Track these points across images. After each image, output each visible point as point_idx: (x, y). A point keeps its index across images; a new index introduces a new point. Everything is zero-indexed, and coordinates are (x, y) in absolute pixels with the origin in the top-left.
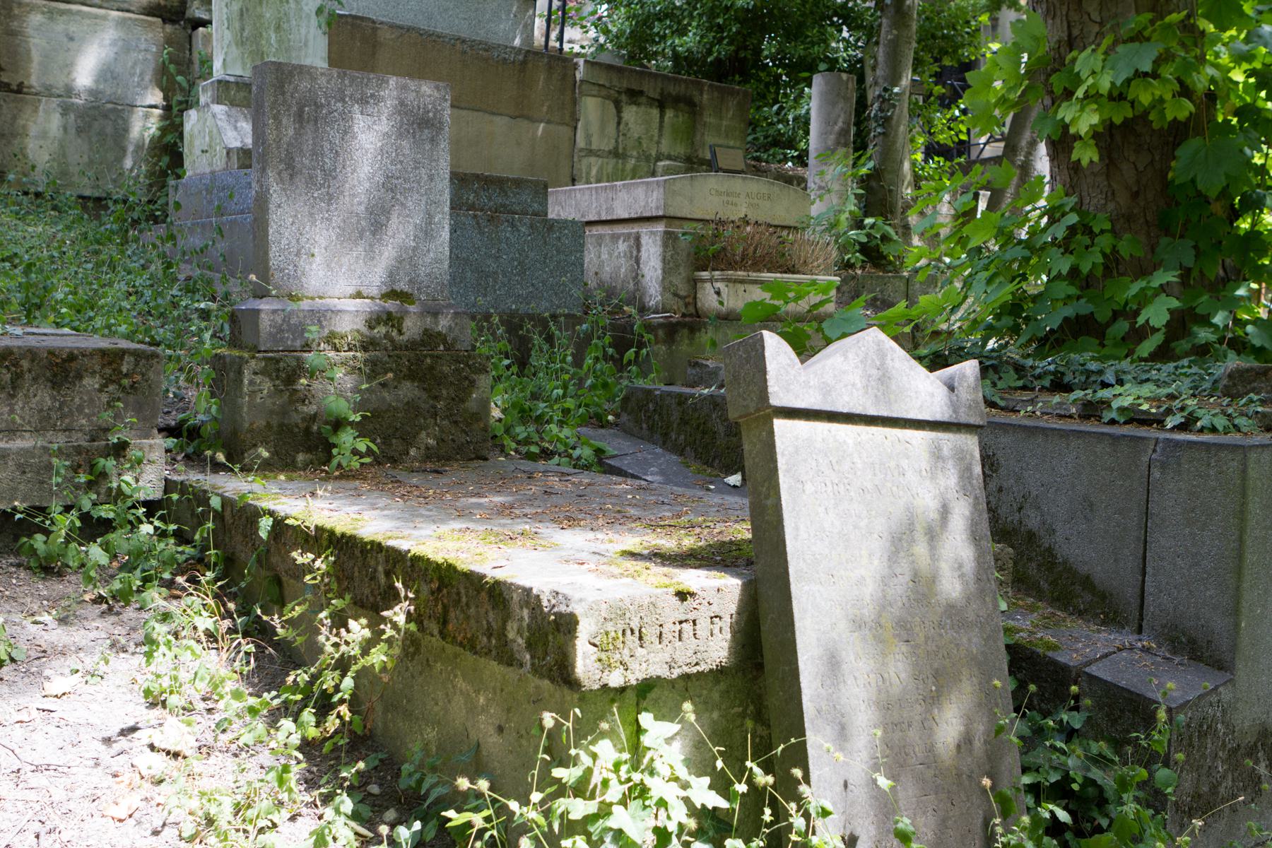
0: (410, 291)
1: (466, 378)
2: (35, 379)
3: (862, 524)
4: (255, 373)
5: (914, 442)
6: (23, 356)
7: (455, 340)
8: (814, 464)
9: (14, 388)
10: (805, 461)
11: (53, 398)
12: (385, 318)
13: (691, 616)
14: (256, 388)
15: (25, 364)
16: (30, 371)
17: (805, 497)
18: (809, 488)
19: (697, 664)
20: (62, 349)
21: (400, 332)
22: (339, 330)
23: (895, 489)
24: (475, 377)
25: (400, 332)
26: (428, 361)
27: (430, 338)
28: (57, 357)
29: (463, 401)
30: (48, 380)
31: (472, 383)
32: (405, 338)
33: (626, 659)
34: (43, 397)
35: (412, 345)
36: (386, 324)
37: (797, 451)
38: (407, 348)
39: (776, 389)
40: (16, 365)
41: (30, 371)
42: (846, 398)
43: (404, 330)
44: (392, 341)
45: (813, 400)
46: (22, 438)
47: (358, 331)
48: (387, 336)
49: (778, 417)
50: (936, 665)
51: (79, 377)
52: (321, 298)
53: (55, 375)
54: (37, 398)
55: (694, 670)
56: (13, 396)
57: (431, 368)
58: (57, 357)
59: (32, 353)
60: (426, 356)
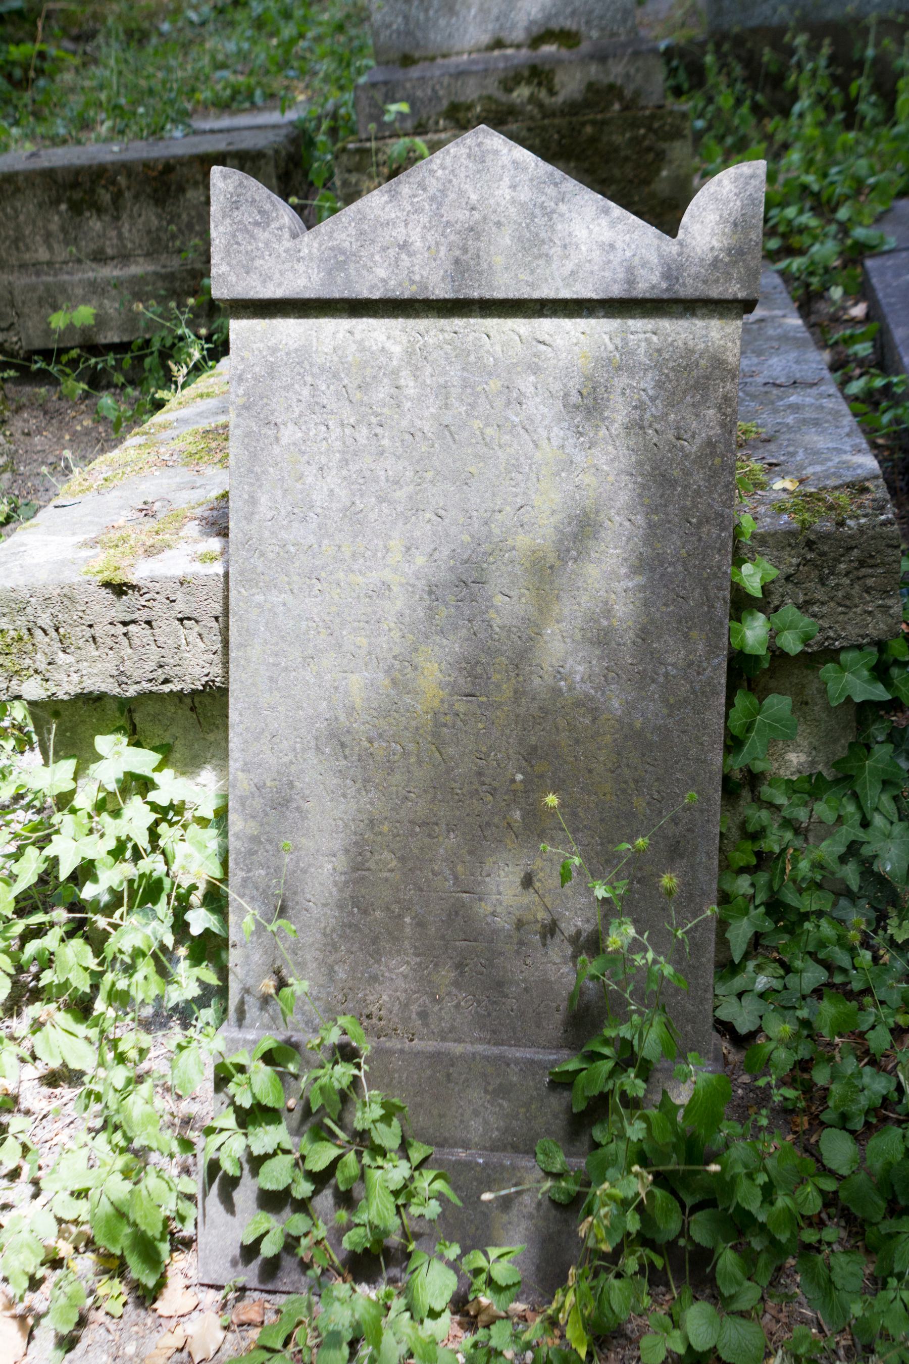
0: (574, 28)
1: (650, 149)
2: (136, 197)
3: (400, 494)
4: (349, 171)
5: (559, 342)
6: (117, 173)
7: (637, 93)
8: (306, 392)
9: (117, 209)
10: (287, 388)
11: (159, 217)
12: (526, 73)
13: (142, 615)
14: (352, 190)
15: (122, 180)
16: (129, 188)
17: (276, 450)
18: (289, 434)
19: (166, 681)
20: (156, 160)
21: (552, 92)
22: (462, 99)
23: (489, 431)
24: (664, 145)
25: (552, 92)
26: (589, 129)
27: (598, 95)
28: (153, 169)
29: (647, 182)
30: (149, 196)
31: (661, 156)
32: (560, 99)
33: (42, 667)
34: (149, 216)
35: (573, 108)
36: (529, 82)
37: (272, 370)
38: (563, 114)
39: (224, 268)
40: (114, 182)
41: (129, 188)
42: (381, 273)
43: (557, 88)
44: (541, 105)
45: (302, 282)
46: (137, 263)
47: (490, 98)
48: (532, 99)
49: (238, 316)
50: (533, 740)
51: (182, 190)
52: (444, 56)
53: (155, 191)
54: (143, 218)
55: (166, 688)
56: (117, 218)
57: (593, 140)
58: (153, 169)
59: (126, 168)
60: (583, 124)
